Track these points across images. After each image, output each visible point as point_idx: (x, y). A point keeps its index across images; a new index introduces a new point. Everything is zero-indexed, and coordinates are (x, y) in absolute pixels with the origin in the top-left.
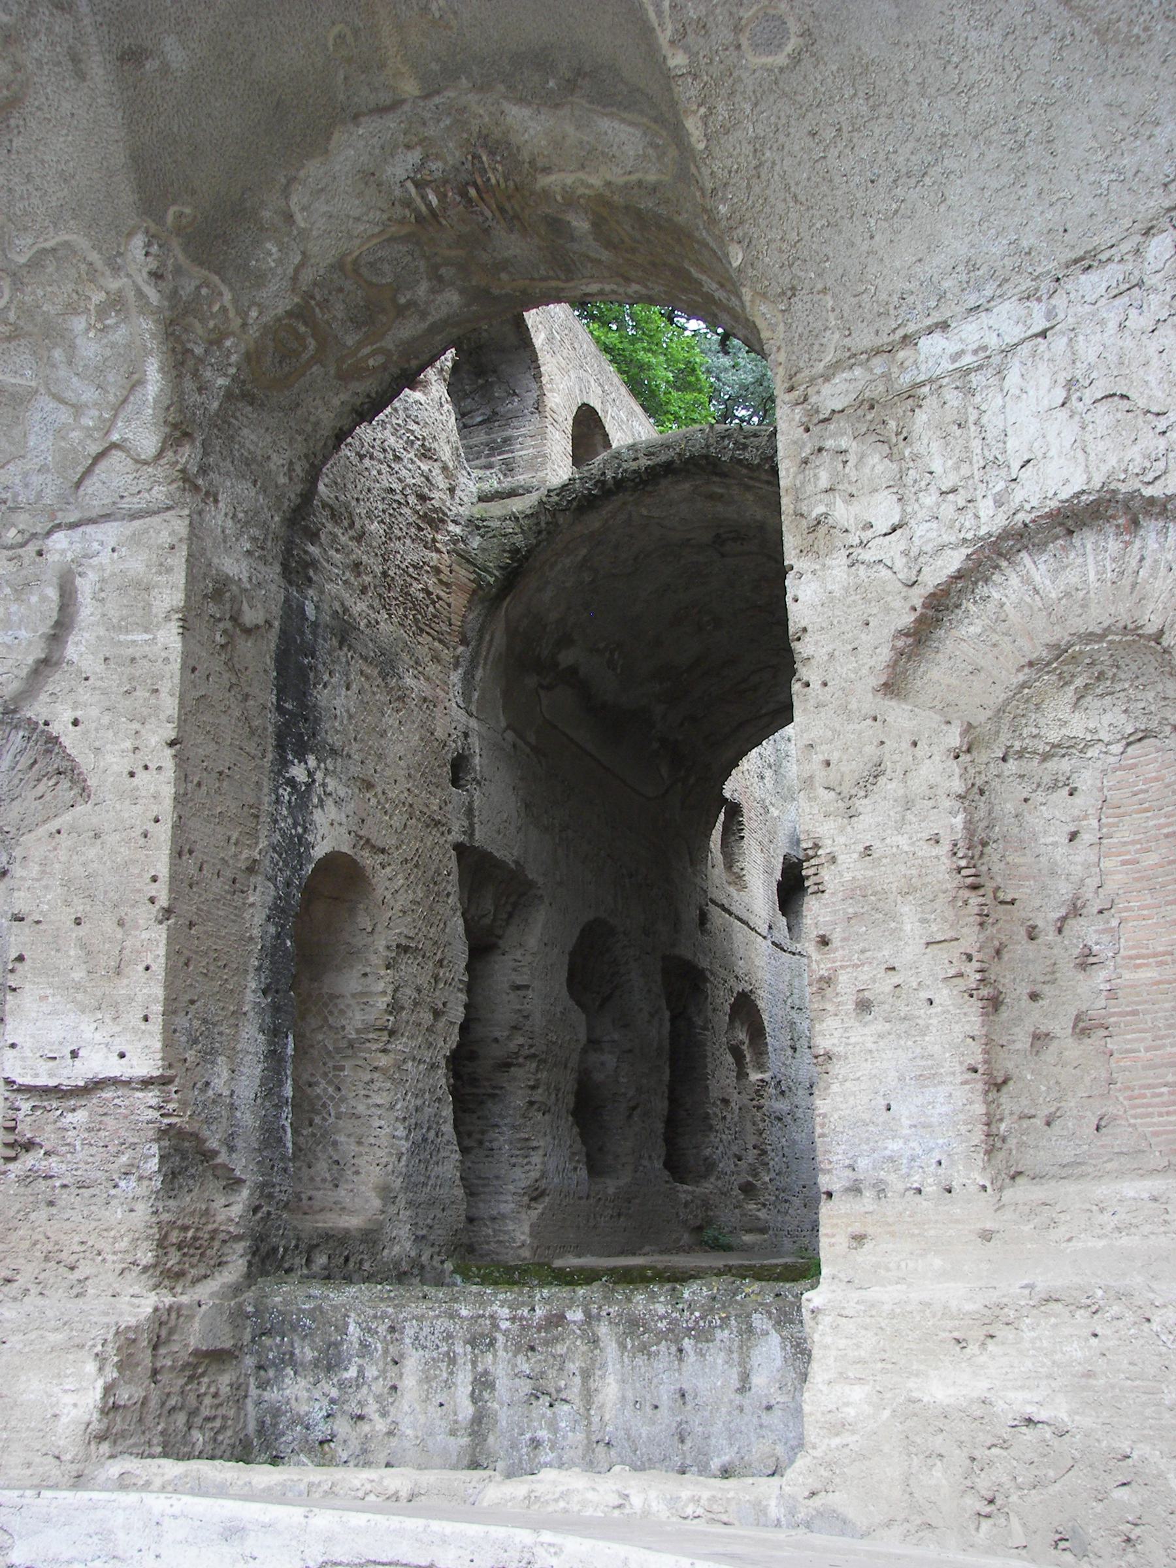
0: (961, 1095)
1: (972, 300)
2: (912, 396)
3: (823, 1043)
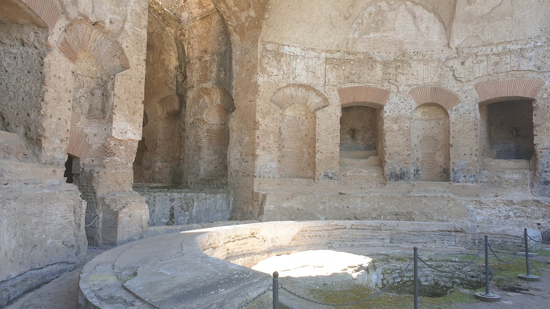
0: (277, 164)
1: (295, 45)
2: (282, 55)
3: (257, 153)
